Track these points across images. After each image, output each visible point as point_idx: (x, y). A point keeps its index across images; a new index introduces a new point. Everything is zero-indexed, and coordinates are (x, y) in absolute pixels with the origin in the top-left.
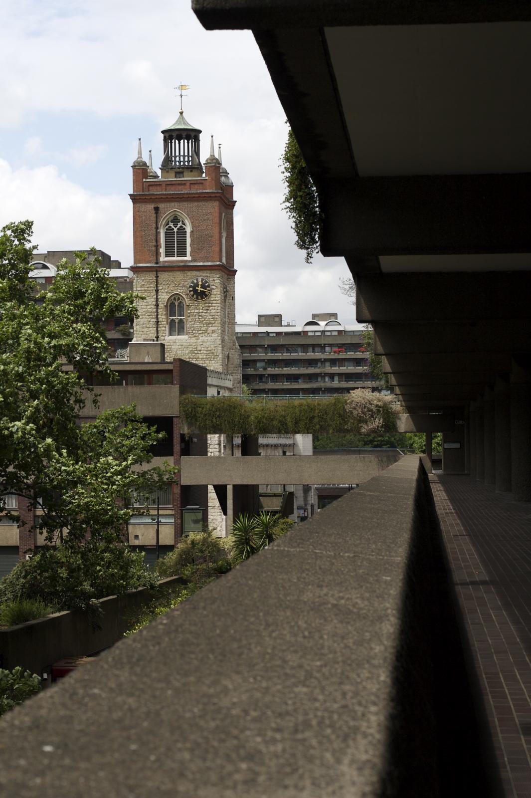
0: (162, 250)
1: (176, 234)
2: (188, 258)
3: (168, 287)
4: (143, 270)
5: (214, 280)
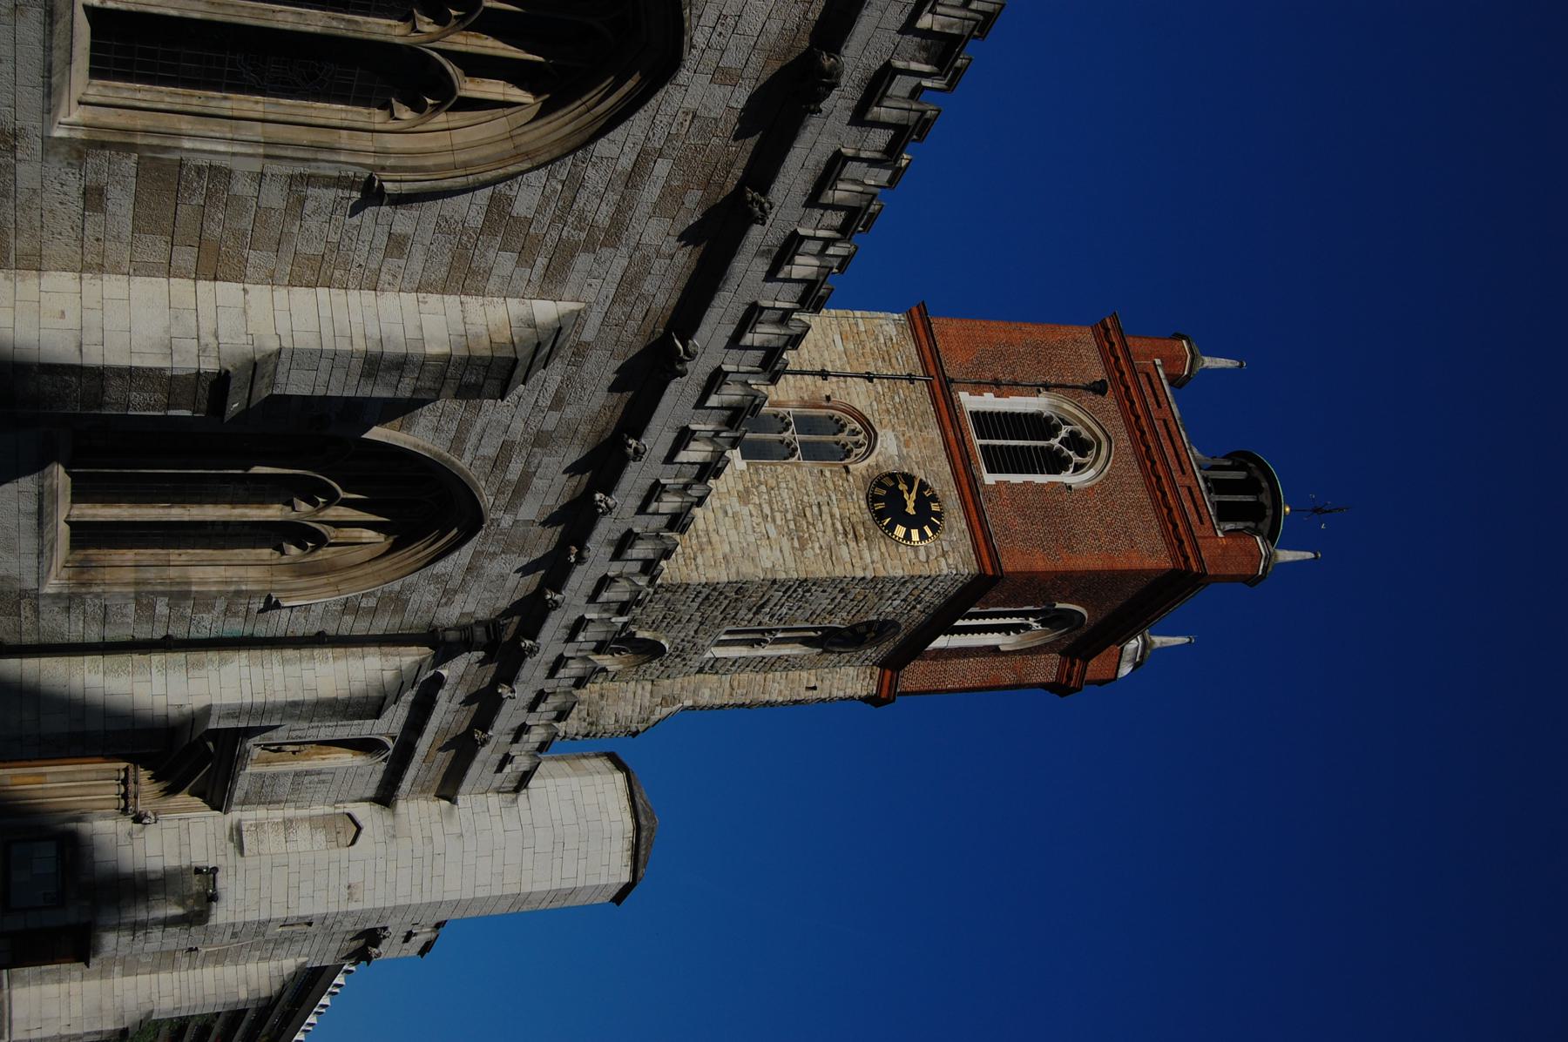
0: (988, 402)
2: (990, 479)
3: (888, 411)
4: (924, 339)
5: (944, 554)
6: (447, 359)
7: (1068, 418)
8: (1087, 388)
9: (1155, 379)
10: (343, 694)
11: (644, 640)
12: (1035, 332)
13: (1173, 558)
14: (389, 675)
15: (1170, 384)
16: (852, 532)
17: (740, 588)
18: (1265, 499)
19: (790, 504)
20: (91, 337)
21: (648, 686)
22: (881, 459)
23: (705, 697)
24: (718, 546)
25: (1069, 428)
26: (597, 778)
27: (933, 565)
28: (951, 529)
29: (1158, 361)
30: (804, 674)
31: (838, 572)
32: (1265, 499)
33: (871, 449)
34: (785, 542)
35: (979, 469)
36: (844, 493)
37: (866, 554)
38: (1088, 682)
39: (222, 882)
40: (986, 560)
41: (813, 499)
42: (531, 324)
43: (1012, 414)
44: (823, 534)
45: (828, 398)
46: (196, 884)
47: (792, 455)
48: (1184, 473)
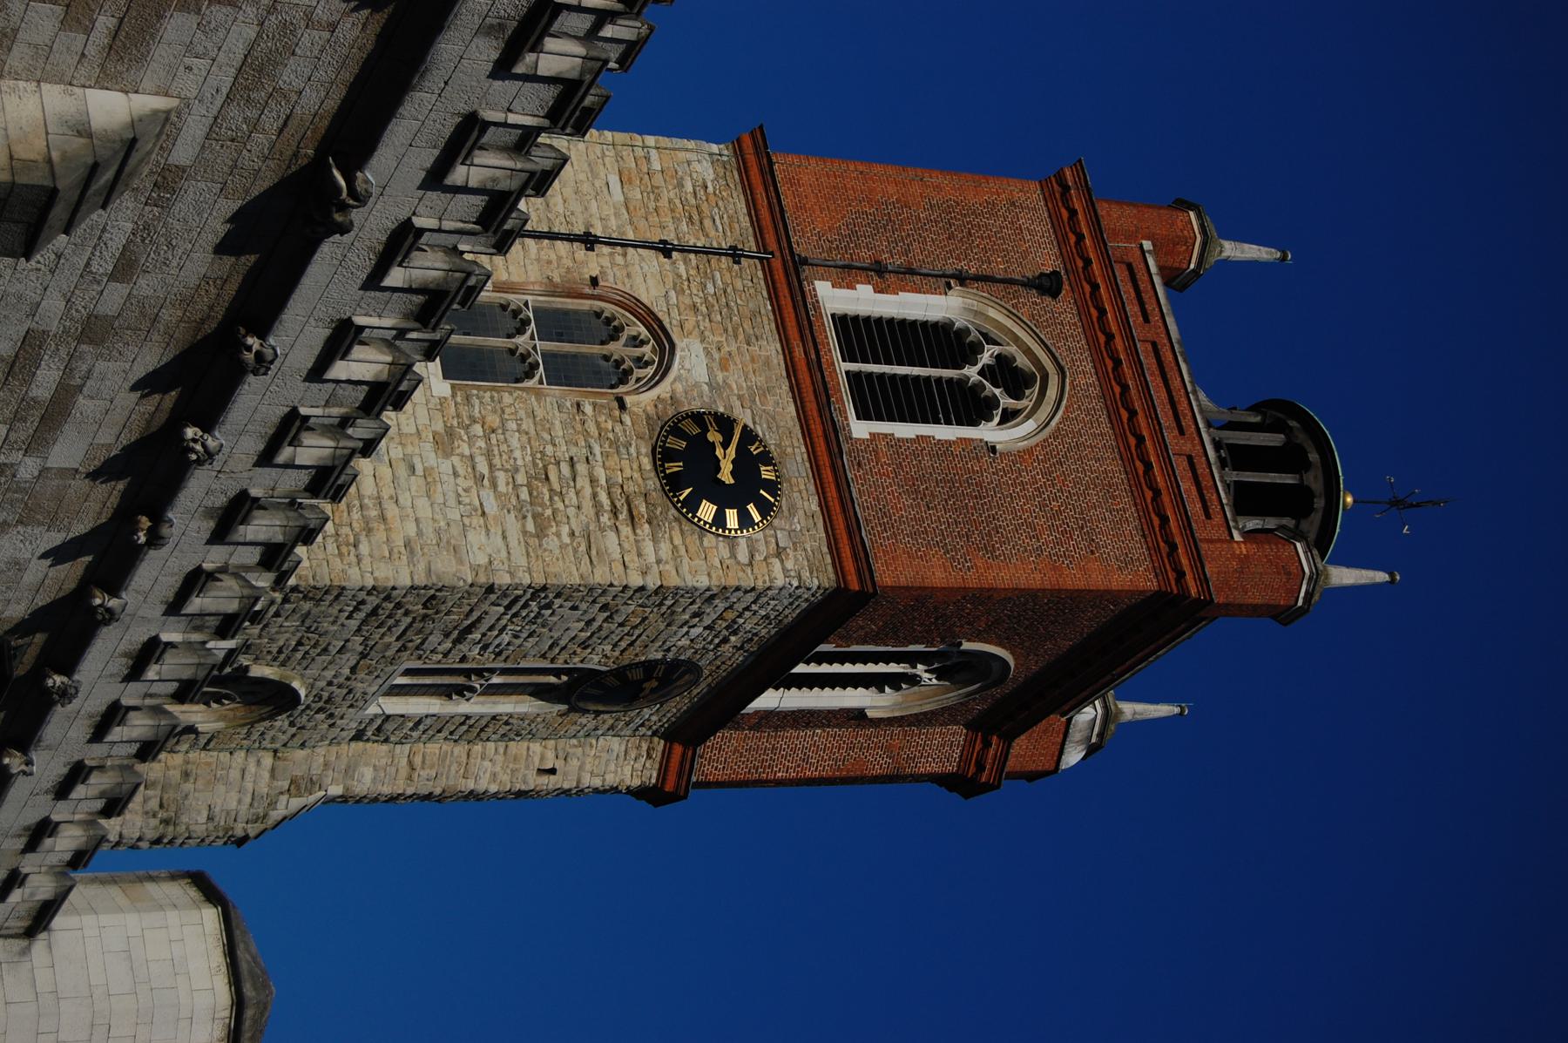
0: (864, 300)
2: (861, 429)
3: (694, 307)
5: (779, 553)
7: (994, 333)
8: (1028, 284)
9: (1141, 276)
11: (263, 682)
12: (945, 186)
13: (1159, 572)
15: (1166, 284)
16: (625, 510)
17: (432, 598)
18: (1314, 480)
19: (521, 457)
21: (268, 760)
22: (679, 387)
23: (365, 781)
24: (396, 524)
25: (996, 350)
26: (172, 917)
27: (760, 569)
28: (793, 510)
29: (1147, 245)
30: (536, 747)
31: (600, 576)
32: (1314, 480)
33: (663, 370)
34: (511, 522)
35: (843, 412)
36: (615, 443)
37: (648, 547)
38: (1014, 776)
40: (849, 565)
41: (563, 451)
42: (83, 130)
43: (903, 322)
44: (576, 512)
45: (594, 281)
47: (529, 375)
48: (1182, 432)
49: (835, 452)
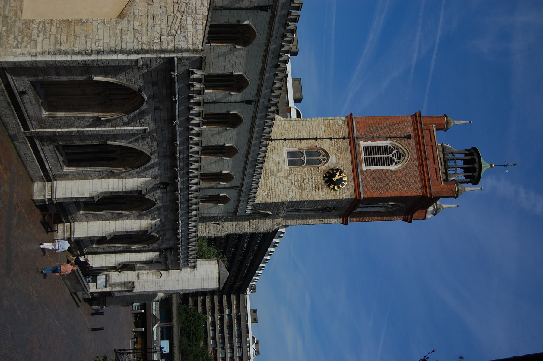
0: (370, 143)
1: (386, 156)
2: (365, 168)
3: (335, 149)
4: (350, 125)
5: (345, 193)
6: (138, 231)
8: (405, 137)
9: (432, 132)
10: (145, 260)
13: (423, 192)
14: (153, 256)
17: (283, 203)
18: (476, 166)
20: (89, 232)
21: (272, 220)
24: (277, 192)
29: (434, 125)
31: (312, 199)
32: (476, 166)
34: (297, 190)
37: (321, 193)
39: (135, 284)
40: (357, 195)
44: (308, 188)
45: (316, 146)
46: (130, 285)
49: (357, 174)
